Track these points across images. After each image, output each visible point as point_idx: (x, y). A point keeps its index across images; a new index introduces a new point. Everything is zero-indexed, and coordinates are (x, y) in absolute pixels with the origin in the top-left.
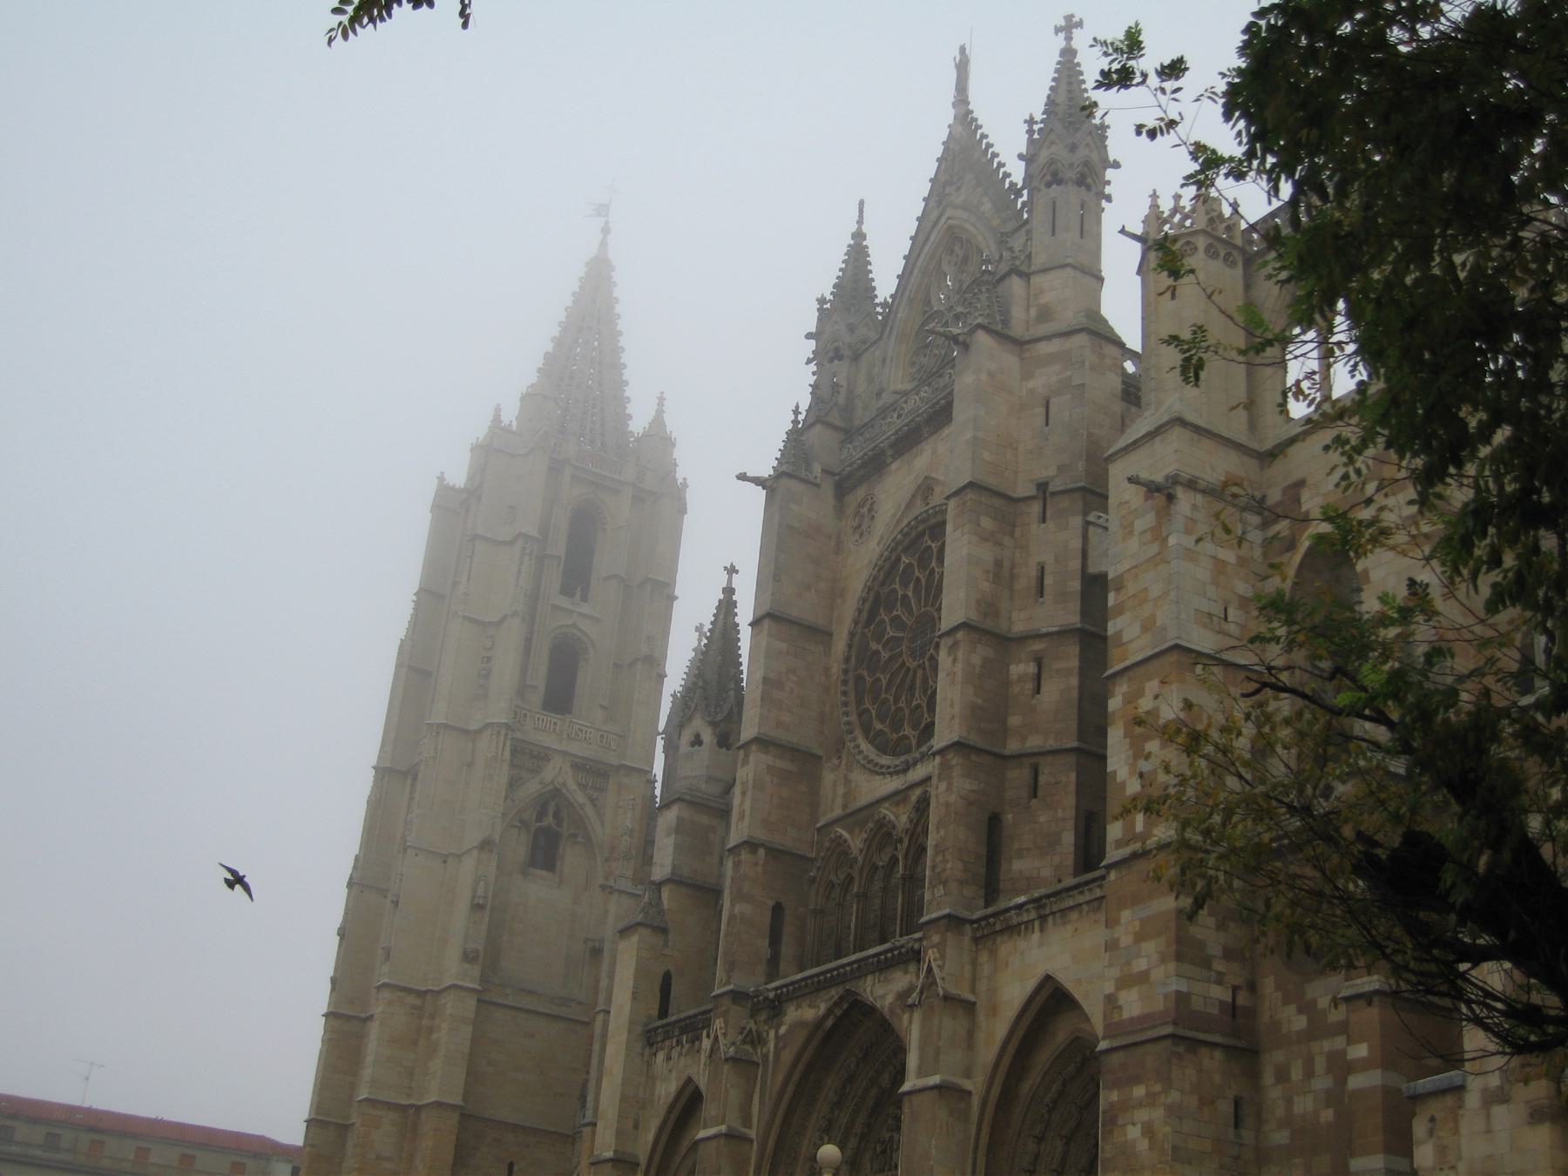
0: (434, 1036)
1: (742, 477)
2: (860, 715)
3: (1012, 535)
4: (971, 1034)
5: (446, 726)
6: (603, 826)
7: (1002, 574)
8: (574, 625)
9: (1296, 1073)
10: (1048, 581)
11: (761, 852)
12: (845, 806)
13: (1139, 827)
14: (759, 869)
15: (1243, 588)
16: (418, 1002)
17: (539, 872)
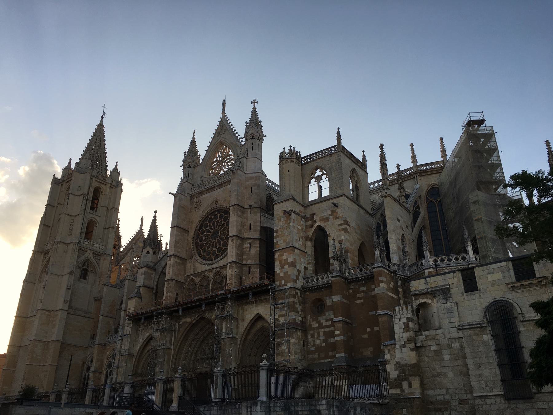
0: (54, 323)
1: (170, 193)
2: (197, 251)
4: (237, 325)
5: (60, 242)
7: (242, 225)
8: (94, 218)
9: (316, 335)
10: (252, 227)
11: (174, 281)
12: (194, 271)
13: (283, 282)
14: (174, 285)
15: (302, 234)
16: (49, 314)
17: (82, 280)
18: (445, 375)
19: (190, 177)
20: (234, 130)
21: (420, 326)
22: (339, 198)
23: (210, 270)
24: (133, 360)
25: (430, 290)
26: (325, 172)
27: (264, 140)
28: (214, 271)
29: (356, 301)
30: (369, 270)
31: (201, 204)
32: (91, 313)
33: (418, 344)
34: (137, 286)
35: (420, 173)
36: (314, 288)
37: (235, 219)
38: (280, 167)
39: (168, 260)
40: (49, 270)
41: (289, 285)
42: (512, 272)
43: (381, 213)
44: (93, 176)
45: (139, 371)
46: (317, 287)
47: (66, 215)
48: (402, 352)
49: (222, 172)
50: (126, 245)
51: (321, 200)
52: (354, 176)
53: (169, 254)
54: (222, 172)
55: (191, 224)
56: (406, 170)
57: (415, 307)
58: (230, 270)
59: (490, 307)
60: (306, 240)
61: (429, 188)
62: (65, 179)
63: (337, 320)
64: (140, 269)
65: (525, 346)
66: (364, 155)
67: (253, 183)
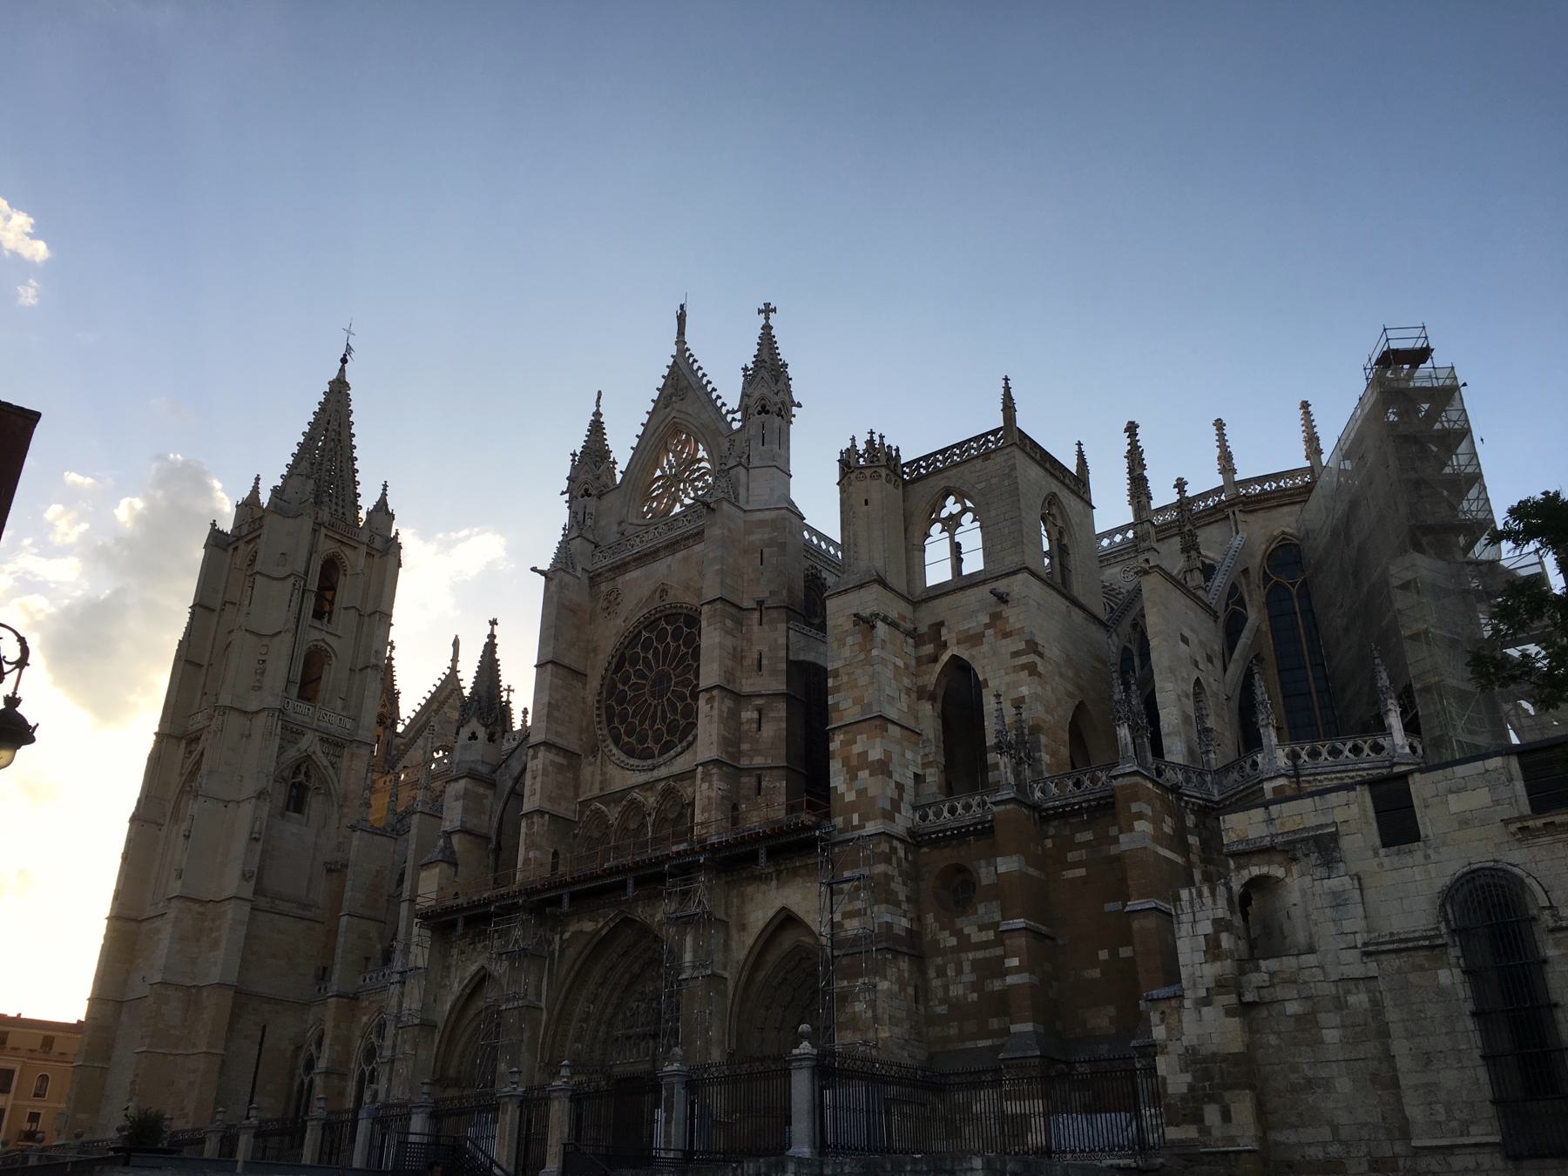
0: (214, 935)
1: (534, 569)
3: (741, 631)
6: (339, 781)
7: (737, 656)
8: (323, 640)
9: (951, 973)
10: (764, 662)
11: (547, 816)
12: (602, 789)
13: (856, 822)
14: (546, 828)
15: (906, 681)
16: (202, 910)
18: (1328, 1084)
19: (589, 522)
20: (709, 388)
21: (1252, 945)
22: (1012, 579)
23: (647, 786)
24: (433, 1039)
25: (1279, 840)
26: (969, 504)
27: (794, 416)
28: (660, 786)
29: (1064, 873)
30: (1100, 784)
31: (619, 600)
32: (318, 908)
33: (1249, 997)
34: (445, 832)
35: (1245, 504)
36: (945, 835)
37: (717, 640)
38: (842, 492)
39: (529, 758)
40: (200, 786)
41: (871, 828)
42: (1519, 786)
43: (1134, 619)
44: (320, 524)
45: (452, 1072)
46: (953, 833)
47: (247, 634)
48: (1201, 1020)
49: (677, 509)
50: (413, 715)
51: (961, 583)
52: (1053, 515)
53: (533, 740)
54: (677, 509)
55: (592, 655)
56: (1204, 496)
57: (1236, 886)
58: (705, 786)
59: (1457, 890)
60: (919, 698)
61: (1273, 546)
62: (244, 532)
63: (1010, 927)
64: (452, 784)
65: (1562, 1003)
66: (1081, 455)
67: (766, 536)
